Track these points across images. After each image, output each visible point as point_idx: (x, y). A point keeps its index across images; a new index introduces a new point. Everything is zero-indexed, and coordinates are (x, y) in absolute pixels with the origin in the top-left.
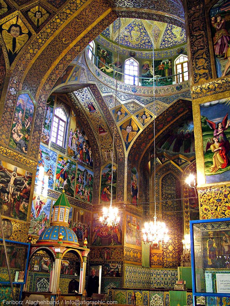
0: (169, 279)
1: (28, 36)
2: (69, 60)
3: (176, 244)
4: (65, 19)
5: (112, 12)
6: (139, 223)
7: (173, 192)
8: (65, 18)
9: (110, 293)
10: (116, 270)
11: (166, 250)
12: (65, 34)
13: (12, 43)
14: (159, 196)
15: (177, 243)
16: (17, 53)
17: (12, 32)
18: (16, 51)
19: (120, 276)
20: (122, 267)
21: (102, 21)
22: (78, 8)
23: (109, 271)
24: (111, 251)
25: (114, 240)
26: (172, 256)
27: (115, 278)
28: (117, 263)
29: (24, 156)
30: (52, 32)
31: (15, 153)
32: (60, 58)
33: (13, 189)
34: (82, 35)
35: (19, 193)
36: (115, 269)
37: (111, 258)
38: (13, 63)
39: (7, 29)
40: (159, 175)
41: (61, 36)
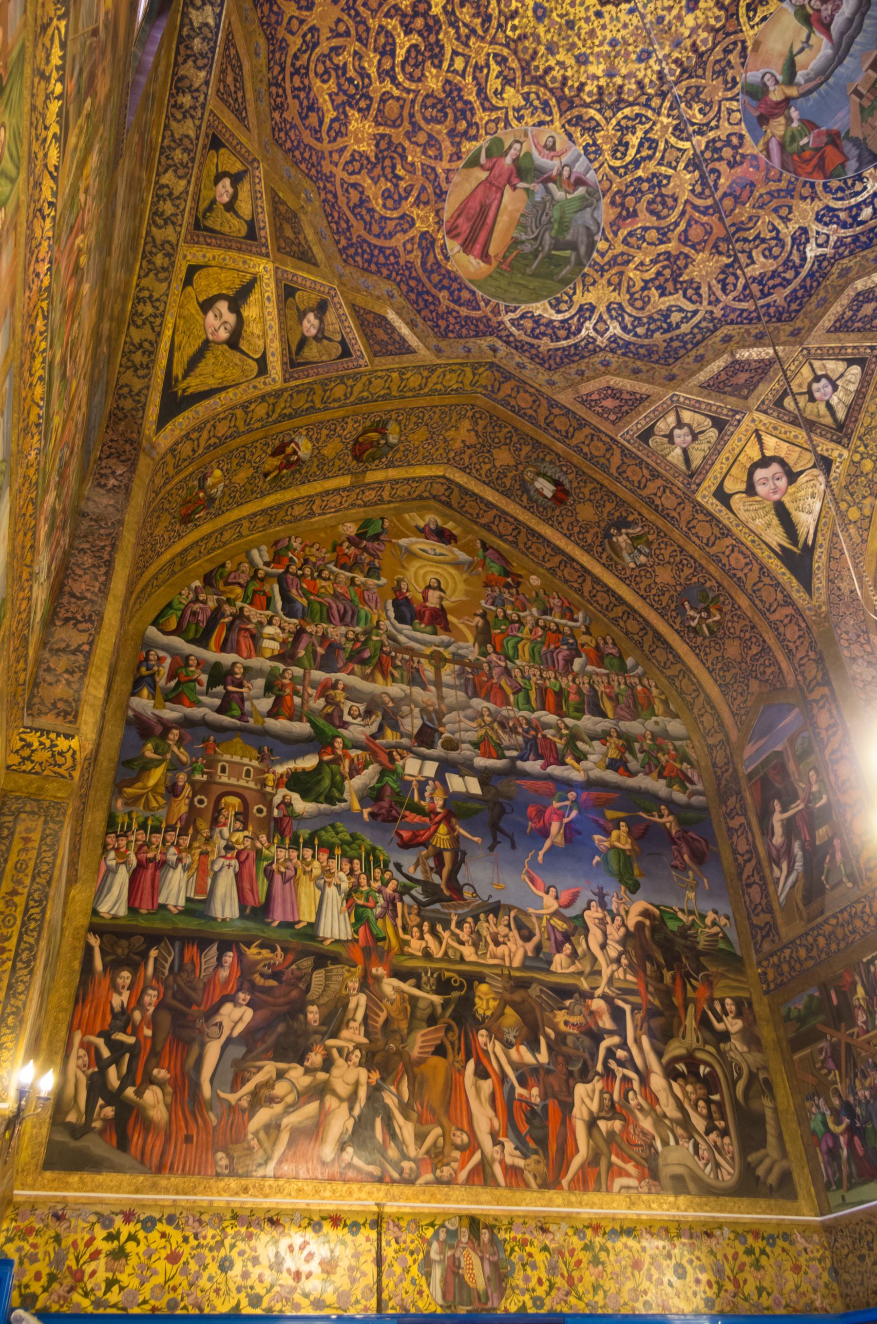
1: (816, 471)
13: (775, 521)
16: (810, 542)
17: (760, 489)
18: (801, 541)
38: (815, 580)
39: (743, 487)
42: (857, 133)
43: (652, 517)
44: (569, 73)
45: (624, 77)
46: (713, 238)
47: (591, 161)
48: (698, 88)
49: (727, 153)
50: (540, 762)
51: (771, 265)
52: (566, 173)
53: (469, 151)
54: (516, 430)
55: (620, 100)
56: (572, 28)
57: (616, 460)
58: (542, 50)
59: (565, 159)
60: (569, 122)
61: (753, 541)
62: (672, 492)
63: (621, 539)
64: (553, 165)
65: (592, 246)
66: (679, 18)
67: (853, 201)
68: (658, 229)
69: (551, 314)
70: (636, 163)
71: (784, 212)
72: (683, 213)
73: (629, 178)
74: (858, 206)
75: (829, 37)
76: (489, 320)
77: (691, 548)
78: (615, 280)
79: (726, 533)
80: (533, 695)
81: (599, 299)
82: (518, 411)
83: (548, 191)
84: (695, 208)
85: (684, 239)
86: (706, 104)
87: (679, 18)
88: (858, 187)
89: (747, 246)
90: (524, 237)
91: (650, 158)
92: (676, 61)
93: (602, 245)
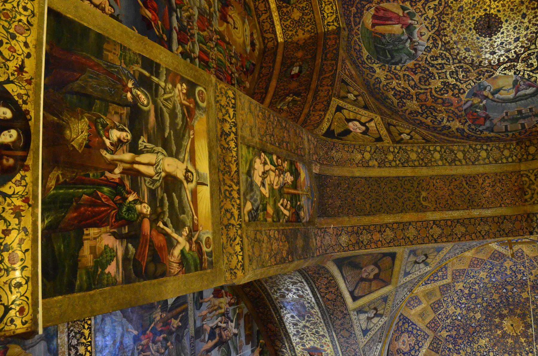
1: (374, 139)
2: (408, 238)
4: (448, 162)
5: (526, 216)
8: (449, 159)
12: (432, 188)
13: (342, 130)
17: (351, 124)
21: (502, 218)
22: (477, 163)
29: (239, 209)
30: (416, 163)
31: (234, 168)
32: (398, 218)
33: (150, 171)
34: (456, 214)
35: (145, 209)
41: (424, 184)
42: (495, 121)
43: (310, 97)
44: (448, 29)
45: (457, 47)
46: (425, 103)
47: (424, 50)
48: (470, 70)
49: (456, 91)
50: (177, 28)
51: (430, 124)
52: (416, 44)
53: (406, 5)
54: (316, 49)
55: (450, 51)
56: (462, 23)
57: (327, 75)
58: (450, 16)
59: (420, 41)
60: (433, 37)
61: (328, 118)
62: (328, 93)
63: (289, 98)
64: (416, 38)
65: (396, 64)
66: (486, 52)
67: (473, 134)
68: (415, 84)
69: (365, 58)
70: (433, 66)
71: (450, 119)
72: (426, 89)
73: (427, 66)
74: (472, 136)
75: (516, 94)
76: (353, 30)
77: (306, 111)
78: (389, 77)
79: (326, 110)
80: (204, 47)
81: (379, 74)
82: (325, 44)
83: (407, 40)
84: (431, 92)
85: (418, 94)
86: (467, 76)
87: (486, 52)
88: (479, 133)
89: (430, 115)
90: (387, 38)
91: (437, 69)
92: (473, 60)
93: (398, 67)
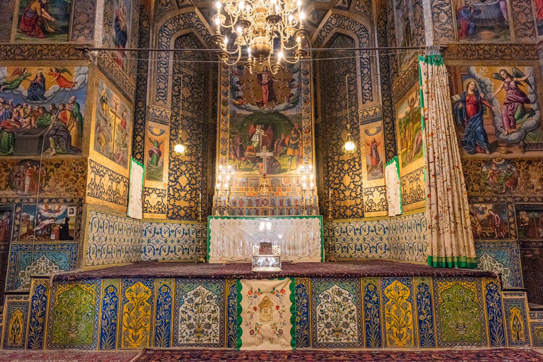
0: (178, 241)
3: (194, 174)
6: (125, 114)
7: (192, 73)
9: (37, 292)
10: (59, 222)
11: (173, 184)
14: (167, 71)
15: (195, 171)
19: (71, 239)
20: (80, 214)
23: (38, 224)
24: (46, 169)
25: (57, 142)
26: (185, 197)
27: (56, 242)
28: (65, 201)
36: (56, 219)
37: (46, 188)
40: (171, 30)
